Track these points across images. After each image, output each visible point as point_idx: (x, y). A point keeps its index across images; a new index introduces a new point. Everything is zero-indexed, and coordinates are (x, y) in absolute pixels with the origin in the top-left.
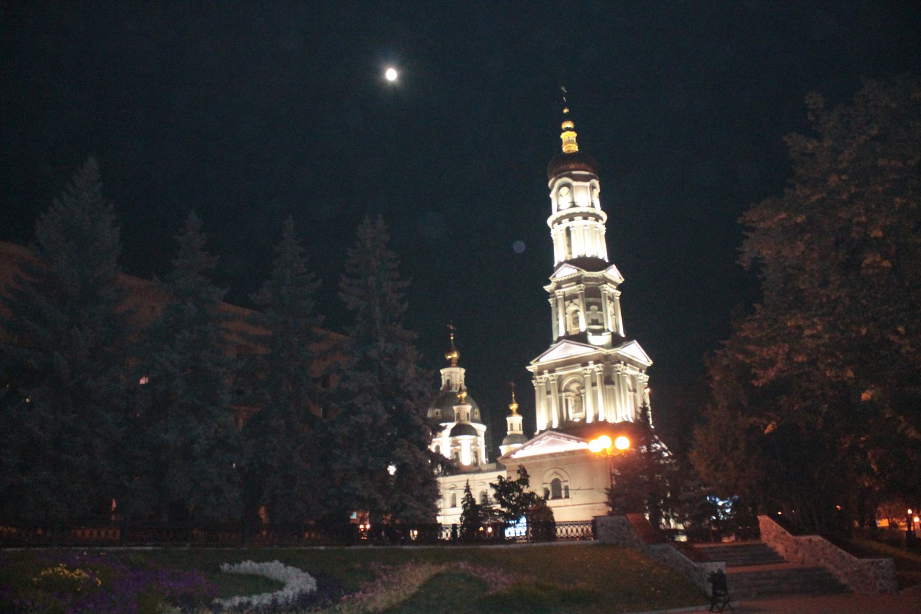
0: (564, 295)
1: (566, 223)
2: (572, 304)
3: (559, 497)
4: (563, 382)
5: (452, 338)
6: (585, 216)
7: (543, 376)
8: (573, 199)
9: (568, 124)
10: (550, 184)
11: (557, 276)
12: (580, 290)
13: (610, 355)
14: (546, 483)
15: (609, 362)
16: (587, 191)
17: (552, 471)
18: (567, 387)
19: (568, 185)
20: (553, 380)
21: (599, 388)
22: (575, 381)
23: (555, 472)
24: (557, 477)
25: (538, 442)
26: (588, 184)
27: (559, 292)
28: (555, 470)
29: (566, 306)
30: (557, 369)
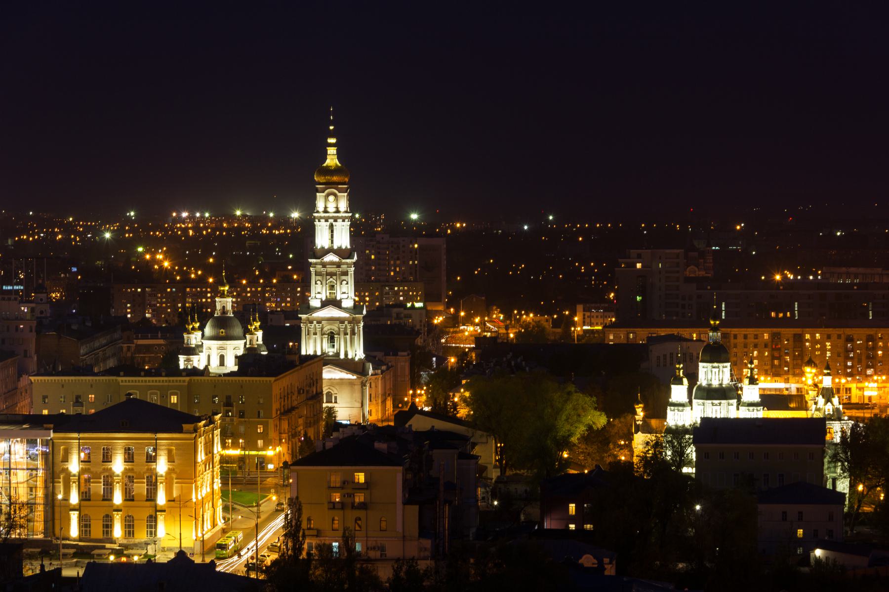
0: (326, 272)
3: (331, 402)
5: (224, 274)
8: (337, 205)
9: (332, 140)
19: (335, 195)
21: (348, 337)
24: (331, 391)
28: (329, 387)
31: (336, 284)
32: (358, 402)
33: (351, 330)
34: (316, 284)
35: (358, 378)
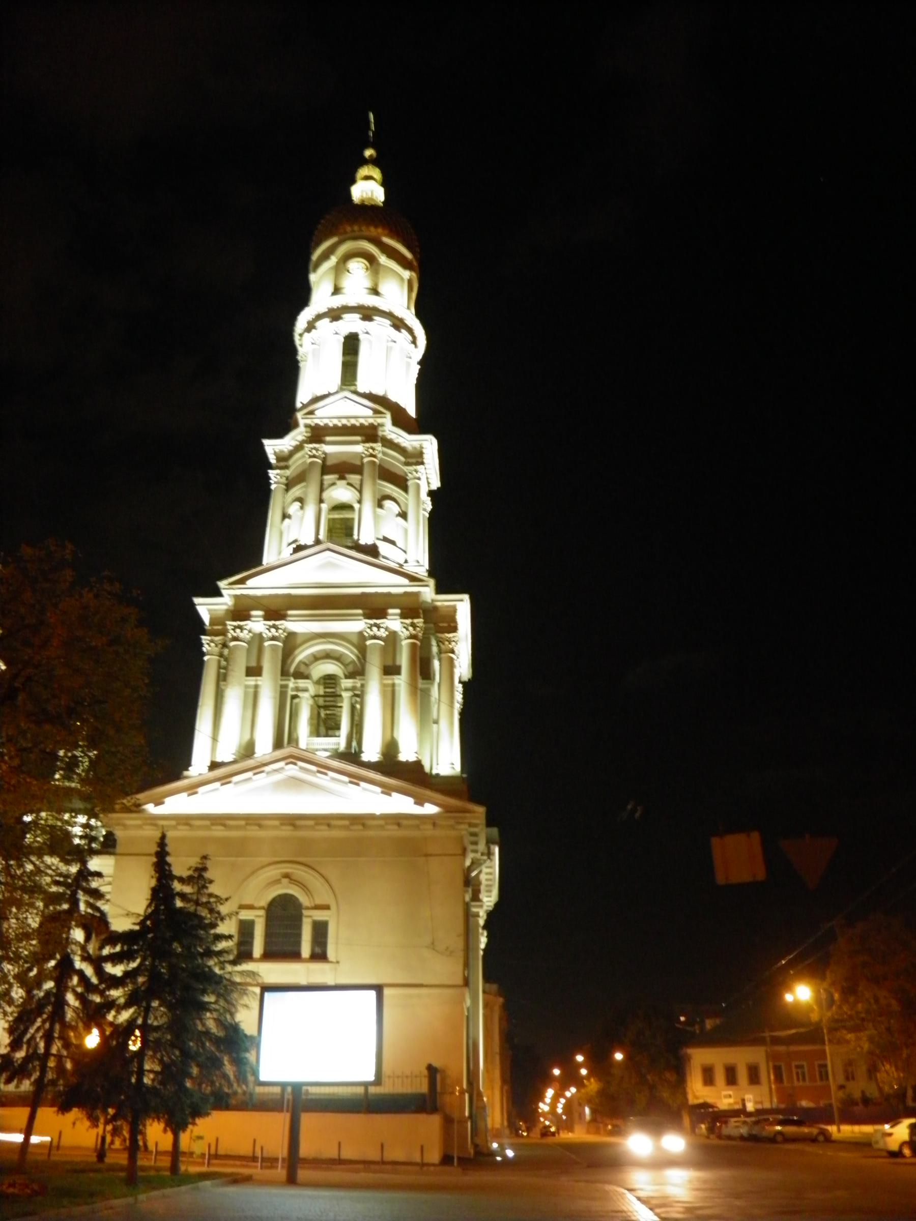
1: (351, 323)
2: (344, 482)
3: (293, 955)
4: (297, 652)
6: (398, 324)
7: (248, 624)
10: (315, 256)
11: (318, 413)
12: (372, 455)
13: (435, 609)
14: (251, 907)
16: (402, 286)
17: (274, 872)
18: (303, 669)
19: (371, 259)
20: (274, 638)
21: (402, 681)
22: (328, 656)
23: (287, 876)
24: (294, 891)
26: (406, 274)
27: (317, 450)
29: (325, 486)
30: (290, 612)
31: (360, 502)
32: (449, 952)
33: (413, 646)
34: (285, 516)
35: (447, 809)
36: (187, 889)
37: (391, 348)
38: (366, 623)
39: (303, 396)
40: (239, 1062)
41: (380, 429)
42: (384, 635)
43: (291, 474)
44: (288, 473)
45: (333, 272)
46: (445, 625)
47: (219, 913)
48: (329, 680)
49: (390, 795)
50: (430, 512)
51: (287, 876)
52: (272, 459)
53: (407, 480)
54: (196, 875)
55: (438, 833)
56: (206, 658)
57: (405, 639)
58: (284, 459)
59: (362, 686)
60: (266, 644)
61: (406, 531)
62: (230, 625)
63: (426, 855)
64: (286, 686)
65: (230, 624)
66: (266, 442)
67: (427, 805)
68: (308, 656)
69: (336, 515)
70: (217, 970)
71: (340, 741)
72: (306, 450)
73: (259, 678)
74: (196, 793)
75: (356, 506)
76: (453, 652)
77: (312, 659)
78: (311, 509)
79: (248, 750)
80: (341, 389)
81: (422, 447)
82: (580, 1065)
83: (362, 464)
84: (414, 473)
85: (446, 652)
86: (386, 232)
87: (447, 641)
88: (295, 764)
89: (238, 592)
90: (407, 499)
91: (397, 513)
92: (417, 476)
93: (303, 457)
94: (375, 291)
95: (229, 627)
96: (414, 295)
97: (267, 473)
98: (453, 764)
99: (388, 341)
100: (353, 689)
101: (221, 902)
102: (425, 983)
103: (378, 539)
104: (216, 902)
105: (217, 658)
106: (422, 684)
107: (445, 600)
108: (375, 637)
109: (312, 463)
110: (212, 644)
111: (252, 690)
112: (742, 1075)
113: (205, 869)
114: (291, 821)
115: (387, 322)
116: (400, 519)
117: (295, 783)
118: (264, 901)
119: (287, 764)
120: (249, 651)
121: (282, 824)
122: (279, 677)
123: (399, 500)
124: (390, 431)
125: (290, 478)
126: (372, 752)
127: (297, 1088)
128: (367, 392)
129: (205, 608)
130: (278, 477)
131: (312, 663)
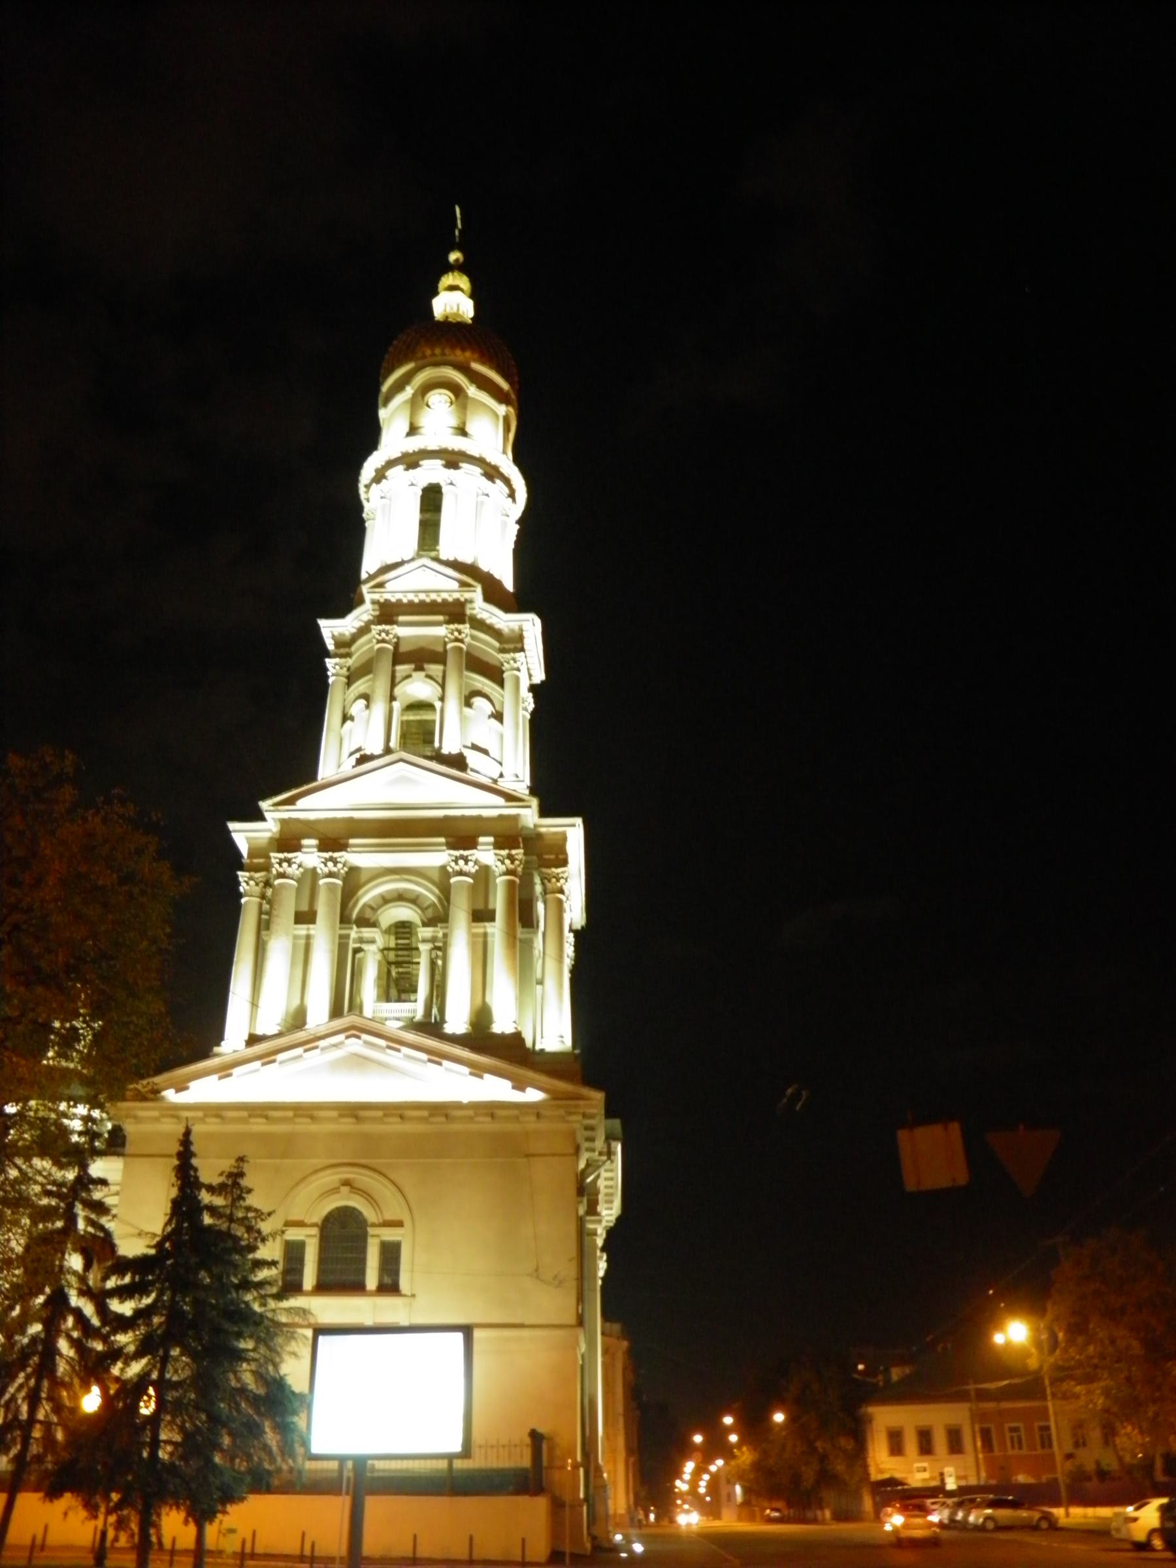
1: (432, 472)
2: (422, 674)
3: (356, 1287)
4: (361, 892)
6: (492, 473)
7: (298, 857)
8: (464, 423)
10: (385, 388)
12: (457, 640)
13: (539, 836)
14: (300, 1224)
15: (535, 858)
16: (497, 426)
17: (330, 1178)
18: (368, 914)
19: (457, 391)
20: (331, 875)
21: (496, 930)
22: (401, 897)
23: (347, 1183)
24: (356, 1202)
25: (299, 1051)
26: (502, 410)
27: (387, 633)
29: (397, 680)
30: (352, 841)
31: (442, 699)
32: (559, 1283)
33: (511, 884)
35: (555, 1096)
36: (219, 1201)
37: (482, 503)
38: (450, 855)
39: (369, 564)
40: (284, 1429)
41: (468, 606)
42: (473, 870)
43: (353, 664)
44: (350, 662)
45: (408, 408)
46: (552, 857)
47: (259, 1232)
48: (402, 929)
49: (481, 1077)
50: (532, 712)
51: (347, 1183)
52: (330, 645)
53: (503, 672)
54: (230, 1182)
55: (543, 1126)
56: (243, 901)
57: (500, 875)
58: (345, 645)
59: (445, 936)
60: (322, 882)
61: (502, 736)
62: (276, 858)
63: (527, 1156)
64: (348, 937)
65: (275, 856)
66: (322, 623)
67: (529, 1090)
68: (374, 897)
69: (412, 717)
70: (256, 1307)
71: (416, 1008)
72: (374, 632)
73: (311, 926)
74: (230, 1075)
75: (438, 705)
76: (562, 891)
77: (380, 901)
78: (379, 708)
79: (298, 1019)
80: (418, 556)
81: (521, 630)
82: (729, 1430)
83: (445, 651)
84: (512, 662)
85: (554, 892)
86: (476, 356)
87: (554, 877)
88: (359, 1037)
89: (286, 815)
90: (502, 696)
91: (490, 713)
92: (515, 665)
93: (370, 641)
94: (462, 431)
95: (273, 861)
96: (512, 436)
97: (324, 663)
98: (562, 1037)
99: (477, 496)
100: (433, 940)
101: (263, 1217)
102: (526, 1323)
103: (465, 747)
104: (255, 1218)
105: (258, 900)
106: (522, 933)
107: (552, 825)
108: (461, 873)
109: (379, 650)
110: (252, 883)
111: (303, 942)
112: (940, 1441)
113: (241, 1175)
114: (353, 1111)
115: (477, 471)
116: (493, 721)
117: (359, 1062)
118: (318, 1216)
119: (347, 1037)
120: (298, 890)
121: (341, 1116)
122: (338, 925)
123: (492, 697)
124: (480, 608)
125: (352, 669)
126: (457, 1022)
127: (360, 1462)
128: (452, 559)
129: (243, 835)
130: (337, 667)
131: (380, 907)
